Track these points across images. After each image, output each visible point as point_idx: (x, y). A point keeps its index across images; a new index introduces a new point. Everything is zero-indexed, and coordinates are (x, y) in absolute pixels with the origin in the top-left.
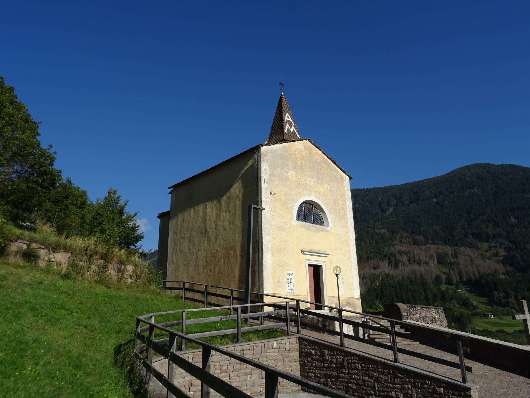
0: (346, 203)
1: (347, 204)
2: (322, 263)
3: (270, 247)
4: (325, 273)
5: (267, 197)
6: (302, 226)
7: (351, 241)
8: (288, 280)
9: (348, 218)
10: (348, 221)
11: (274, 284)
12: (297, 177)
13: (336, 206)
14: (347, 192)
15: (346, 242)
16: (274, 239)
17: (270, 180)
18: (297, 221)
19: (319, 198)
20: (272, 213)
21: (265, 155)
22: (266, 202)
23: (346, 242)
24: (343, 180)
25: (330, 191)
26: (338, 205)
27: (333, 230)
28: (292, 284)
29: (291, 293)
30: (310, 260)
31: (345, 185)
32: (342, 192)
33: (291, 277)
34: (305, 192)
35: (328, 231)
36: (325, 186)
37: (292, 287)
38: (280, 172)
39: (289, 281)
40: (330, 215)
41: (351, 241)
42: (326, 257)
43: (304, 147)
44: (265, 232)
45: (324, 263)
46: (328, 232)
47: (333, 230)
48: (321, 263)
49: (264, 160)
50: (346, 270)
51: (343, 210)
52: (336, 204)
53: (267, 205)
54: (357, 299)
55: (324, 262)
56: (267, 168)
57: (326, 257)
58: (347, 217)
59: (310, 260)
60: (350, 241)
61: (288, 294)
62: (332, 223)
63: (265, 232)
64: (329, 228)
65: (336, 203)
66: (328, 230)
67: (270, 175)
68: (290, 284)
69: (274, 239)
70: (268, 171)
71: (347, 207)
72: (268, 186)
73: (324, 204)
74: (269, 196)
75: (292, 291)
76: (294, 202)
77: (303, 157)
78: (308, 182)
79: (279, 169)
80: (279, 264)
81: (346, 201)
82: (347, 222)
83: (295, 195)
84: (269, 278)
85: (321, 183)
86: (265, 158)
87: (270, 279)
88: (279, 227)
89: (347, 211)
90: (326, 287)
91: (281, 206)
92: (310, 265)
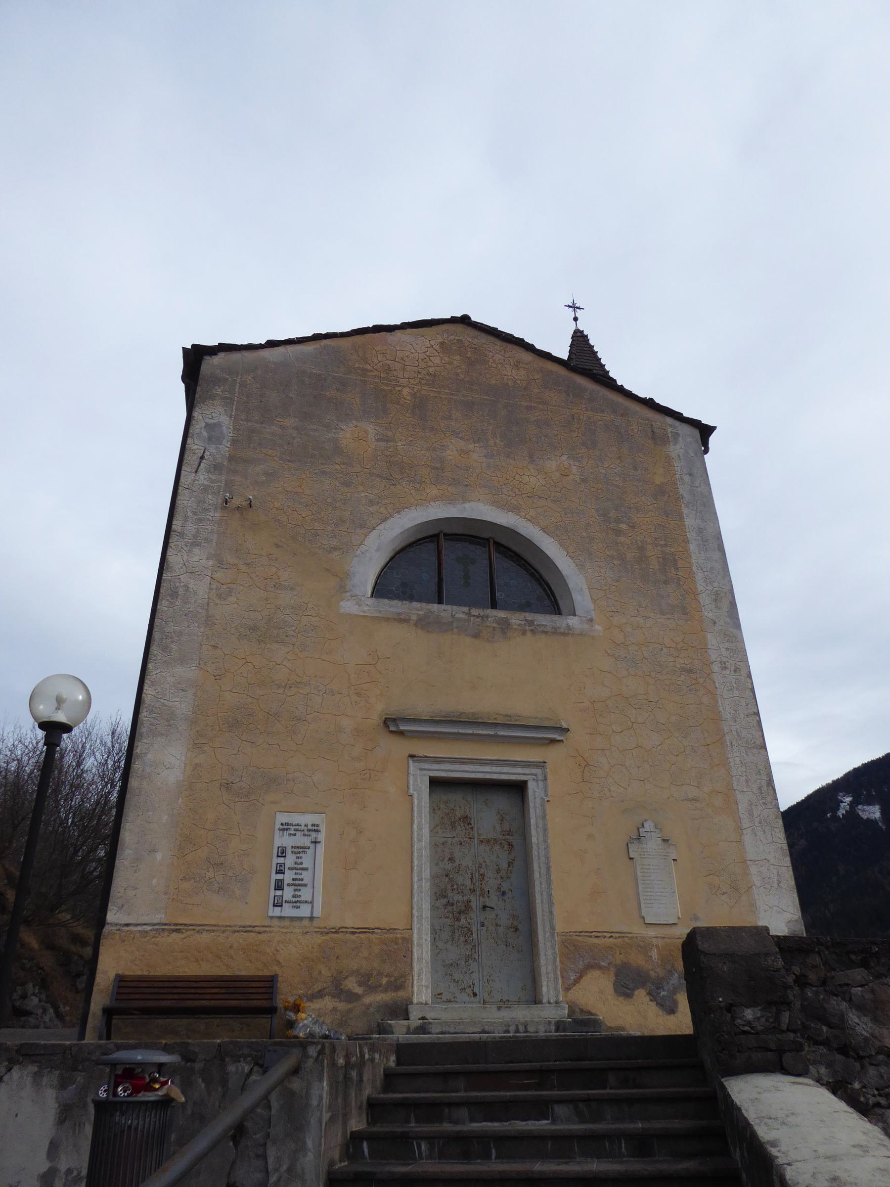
0: (681, 518)
2: (527, 771)
3: (182, 705)
4: (544, 817)
5: (200, 520)
6: (401, 620)
8: (282, 853)
9: (699, 576)
10: (700, 588)
12: (387, 440)
13: (618, 532)
14: (687, 478)
15: (690, 671)
16: (218, 677)
17: (231, 458)
18: (371, 601)
19: (515, 509)
20: (218, 575)
22: (195, 537)
23: (690, 671)
25: (584, 481)
27: (598, 627)
28: (306, 876)
29: (292, 919)
30: (437, 760)
31: (673, 455)
33: (306, 841)
34: (433, 491)
35: (568, 632)
36: (551, 465)
37: (305, 894)
38: (296, 428)
39: (290, 861)
40: (581, 567)
42: (553, 741)
46: (564, 634)
48: (519, 770)
49: (212, 398)
50: (695, 800)
51: (666, 545)
52: (623, 526)
53: (196, 550)
55: (542, 765)
56: (225, 420)
57: (553, 741)
58: (692, 574)
59: (437, 760)
60: (716, 667)
61: (276, 922)
62: (594, 601)
63: (165, 649)
64: (573, 621)
65: (618, 521)
66: (569, 627)
67: (234, 442)
68: (288, 877)
69: (218, 677)
71: (691, 535)
72: (213, 481)
73: (544, 529)
75: (304, 911)
76: (362, 527)
77: (429, 374)
78: (450, 455)
80: (227, 786)
81: (685, 511)
83: (371, 503)
84: (154, 851)
85: (531, 456)
86: (218, 391)
87: (159, 856)
88: (254, 628)
89: (692, 547)
90: (549, 883)
91: (277, 546)
92: (436, 783)
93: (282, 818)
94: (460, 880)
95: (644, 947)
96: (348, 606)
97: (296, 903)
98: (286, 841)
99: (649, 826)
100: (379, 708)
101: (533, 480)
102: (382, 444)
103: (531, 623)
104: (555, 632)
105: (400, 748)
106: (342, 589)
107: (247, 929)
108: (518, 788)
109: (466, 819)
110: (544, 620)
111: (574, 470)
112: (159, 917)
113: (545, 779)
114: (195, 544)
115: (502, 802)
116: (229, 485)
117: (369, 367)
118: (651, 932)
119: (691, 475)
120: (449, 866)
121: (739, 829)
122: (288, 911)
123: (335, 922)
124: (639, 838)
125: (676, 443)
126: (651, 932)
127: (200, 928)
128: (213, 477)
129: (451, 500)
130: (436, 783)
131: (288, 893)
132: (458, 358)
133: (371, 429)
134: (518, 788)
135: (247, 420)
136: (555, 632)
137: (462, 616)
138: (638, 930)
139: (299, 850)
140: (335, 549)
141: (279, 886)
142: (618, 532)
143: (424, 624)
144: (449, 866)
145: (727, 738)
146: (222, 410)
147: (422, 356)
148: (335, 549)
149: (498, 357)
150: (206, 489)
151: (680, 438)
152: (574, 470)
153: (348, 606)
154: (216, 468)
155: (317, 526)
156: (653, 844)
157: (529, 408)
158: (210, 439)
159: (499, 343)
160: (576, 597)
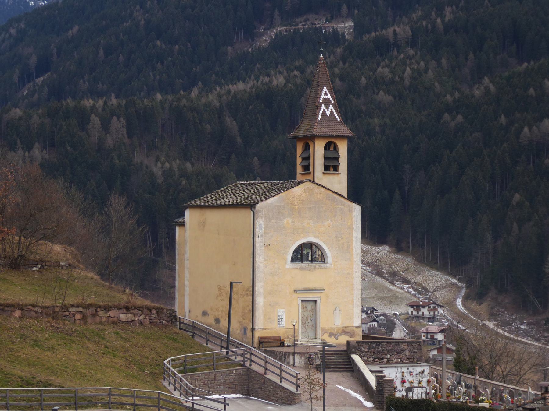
1: (355, 235)
3: (262, 290)
4: (320, 307)
7: (356, 273)
8: (279, 316)
9: (354, 250)
10: (354, 253)
11: (265, 321)
14: (355, 222)
15: (349, 274)
16: (267, 284)
17: (264, 233)
21: (259, 211)
23: (349, 274)
24: (351, 211)
25: (333, 227)
26: (342, 239)
27: (332, 266)
28: (283, 320)
30: (303, 297)
32: (349, 224)
33: (282, 314)
34: (302, 235)
36: (326, 223)
39: (280, 317)
40: (330, 251)
41: (356, 273)
43: (304, 189)
44: (258, 279)
45: (319, 298)
46: (326, 268)
47: (332, 266)
49: (259, 217)
53: (260, 257)
54: (356, 327)
55: (320, 297)
56: (262, 222)
58: (353, 250)
59: (303, 297)
60: (354, 273)
64: (328, 265)
65: (339, 237)
66: (327, 266)
67: (264, 228)
68: (280, 320)
70: (263, 226)
71: (354, 239)
74: (263, 248)
75: (283, 326)
76: (289, 247)
77: (302, 200)
79: (274, 221)
80: (270, 305)
81: (354, 232)
82: (353, 254)
83: (290, 240)
84: (260, 317)
88: (271, 273)
89: (354, 242)
91: (274, 254)
92: (302, 301)
93: (279, 310)
94: (304, 318)
95: (334, 329)
96: (287, 267)
97: (282, 324)
98: (279, 314)
99: (337, 308)
100: (293, 288)
101: (322, 229)
102: (292, 224)
103: (320, 266)
104: (324, 268)
105: (296, 295)
106: (286, 263)
107: (275, 329)
108: (315, 301)
109: (306, 307)
110: (322, 265)
111: (331, 224)
112: (263, 328)
113: (320, 300)
114: (260, 256)
115: (312, 303)
116: (264, 240)
117: (289, 201)
118: (335, 327)
119: (357, 221)
120: (303, 316)
121: (353, 307)
122: (280, 326)
123: (287, 327)
124: (335, 310)
125: (355, 211)
126: (335, 327)
127: (269, 329)
128: (261, 238)
129: (305, 237)
130: (302, 301)
131: (280, 323)
132: (308, 194)
133: (290, 220)
134: (315, 301)
135: (266, 222)
136: (324, 268)
137: (307, 266)
138: (333, 326)
139: (282, 315)
140: (284, 253)
141: (279, 322)
142: (339, 241)
143: (301, 269)
144: (303, 316)
145: (354, 288)
146: (261, 220)
147: (300, 195)
148: (284, 253)
149: (317, 191)
150: (260, 242)
151: (356, 210)
152: (331, 224)
153: (287, 267)
154: (262, 236)
155: (281, 248)
156: (338, 311)
157: (322, 207)
158: (260, 228)
159: (317, 186)
160: (329, 259)
